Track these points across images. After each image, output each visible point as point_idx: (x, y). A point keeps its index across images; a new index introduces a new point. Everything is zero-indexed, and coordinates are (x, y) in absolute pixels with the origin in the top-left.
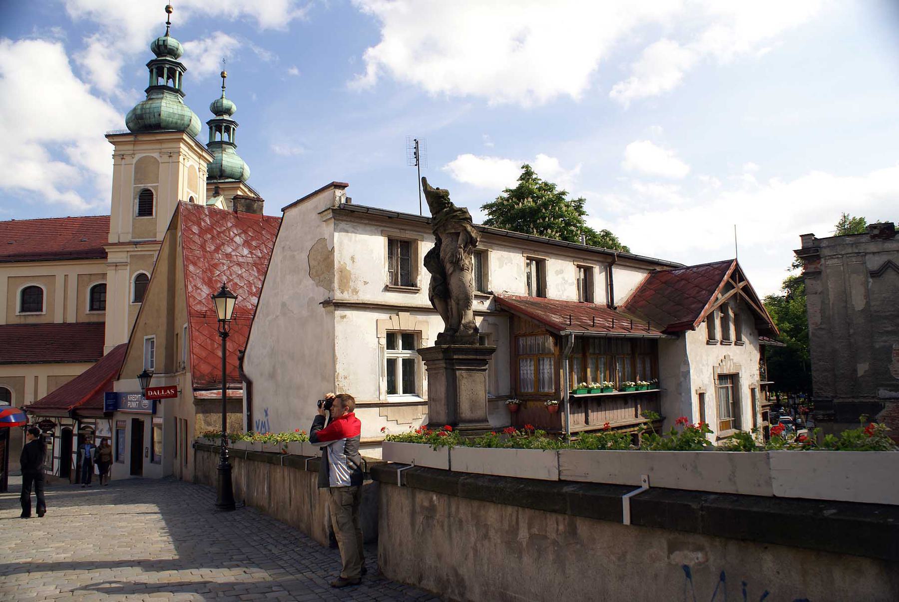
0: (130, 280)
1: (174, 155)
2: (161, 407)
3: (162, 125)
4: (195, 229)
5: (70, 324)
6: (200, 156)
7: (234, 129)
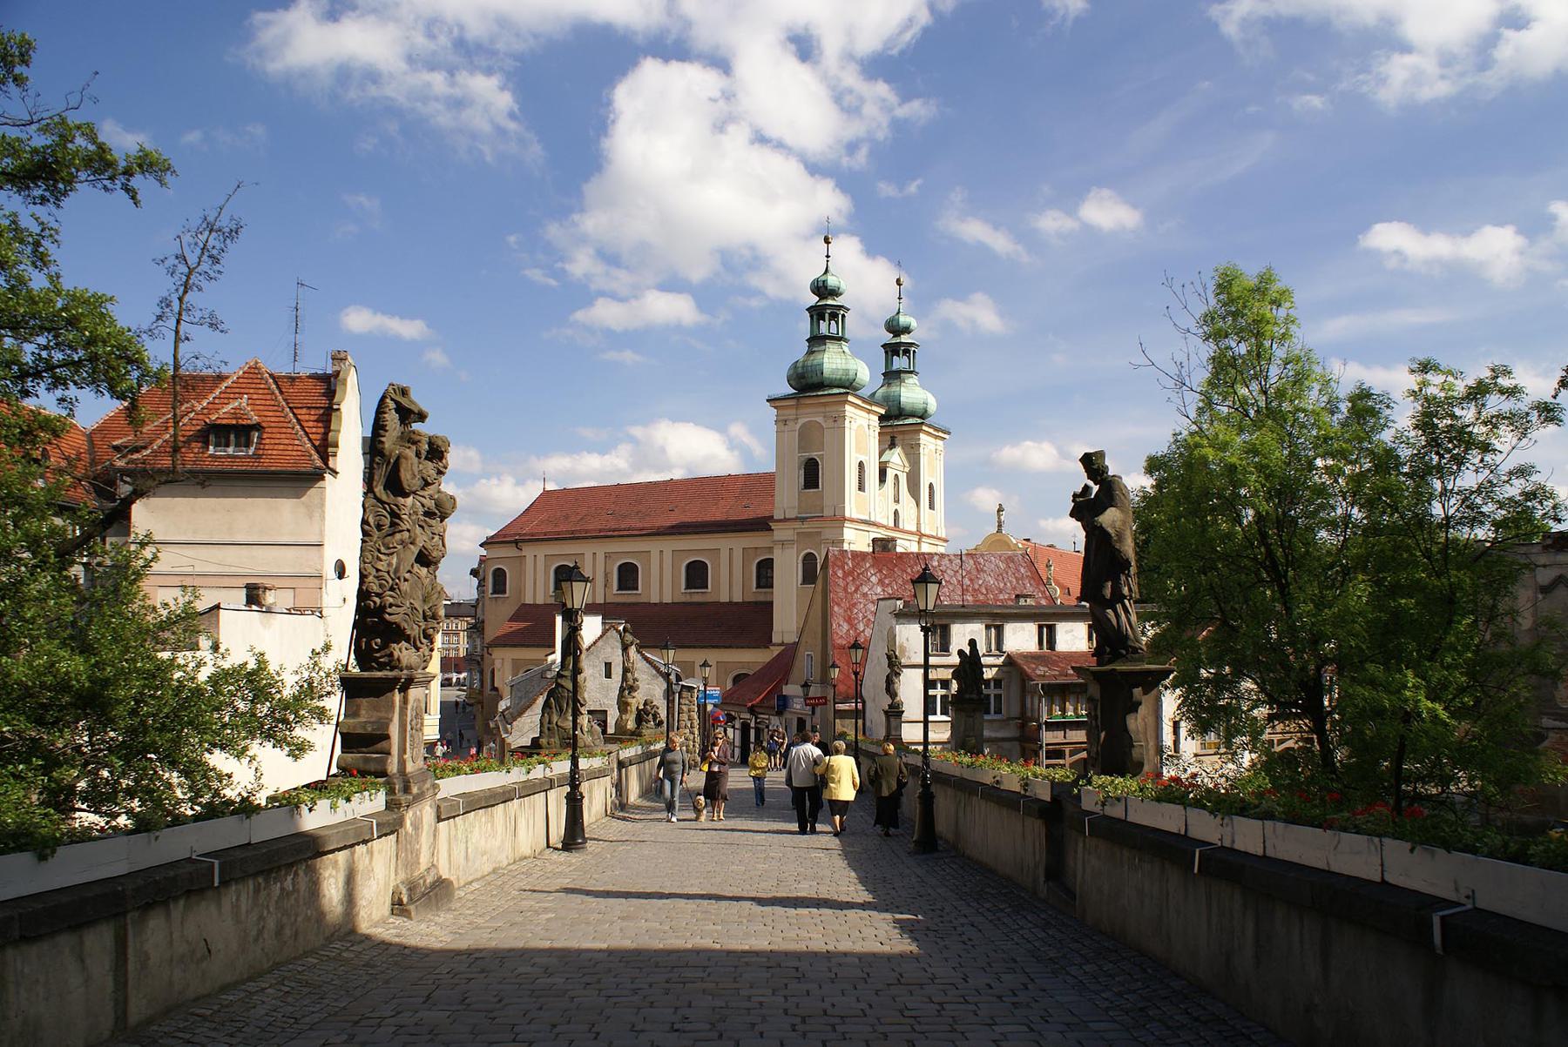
1: (839, 419)
2: (818, 710)
3: (825, 384)
4: (840, 573)
5: (736, 603)
6: (869, 411)
7: (914, 352)
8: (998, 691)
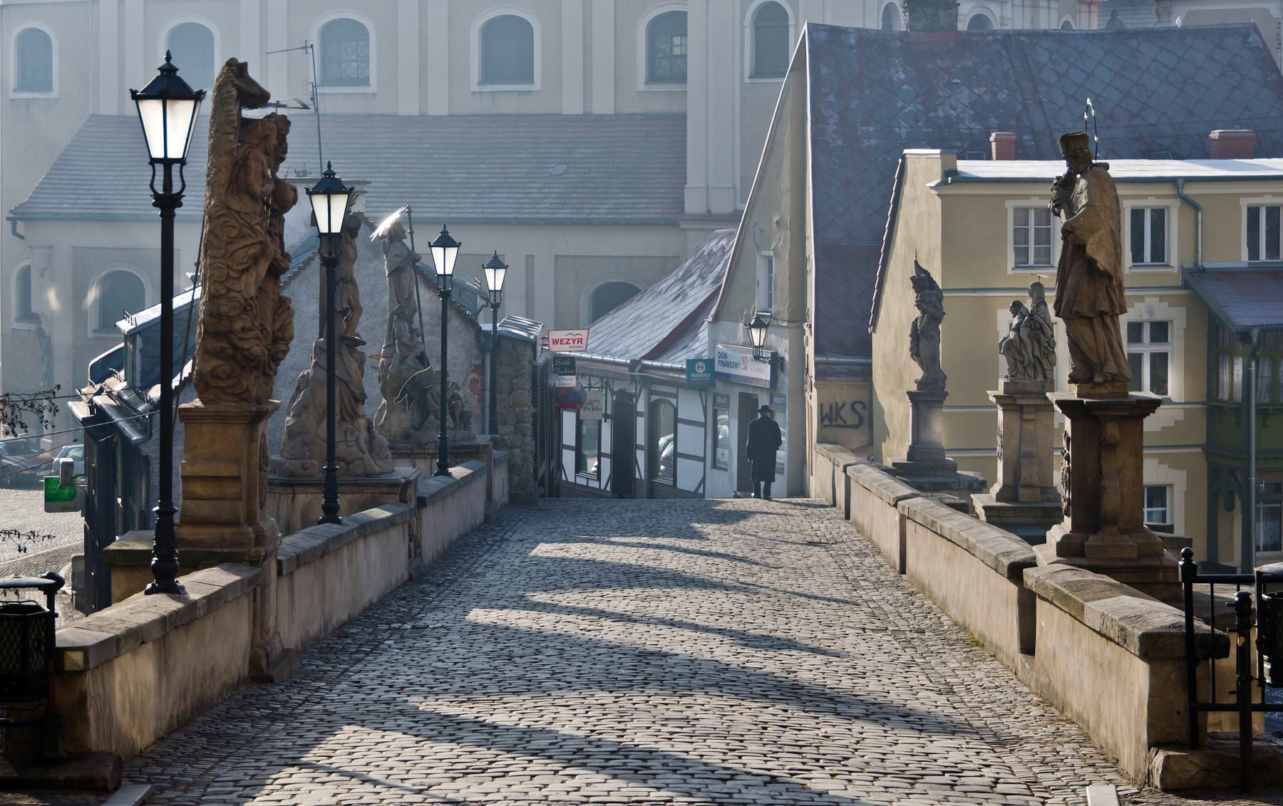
0: (743, 18)
5: (601, 118)
8: (1159, 348)
